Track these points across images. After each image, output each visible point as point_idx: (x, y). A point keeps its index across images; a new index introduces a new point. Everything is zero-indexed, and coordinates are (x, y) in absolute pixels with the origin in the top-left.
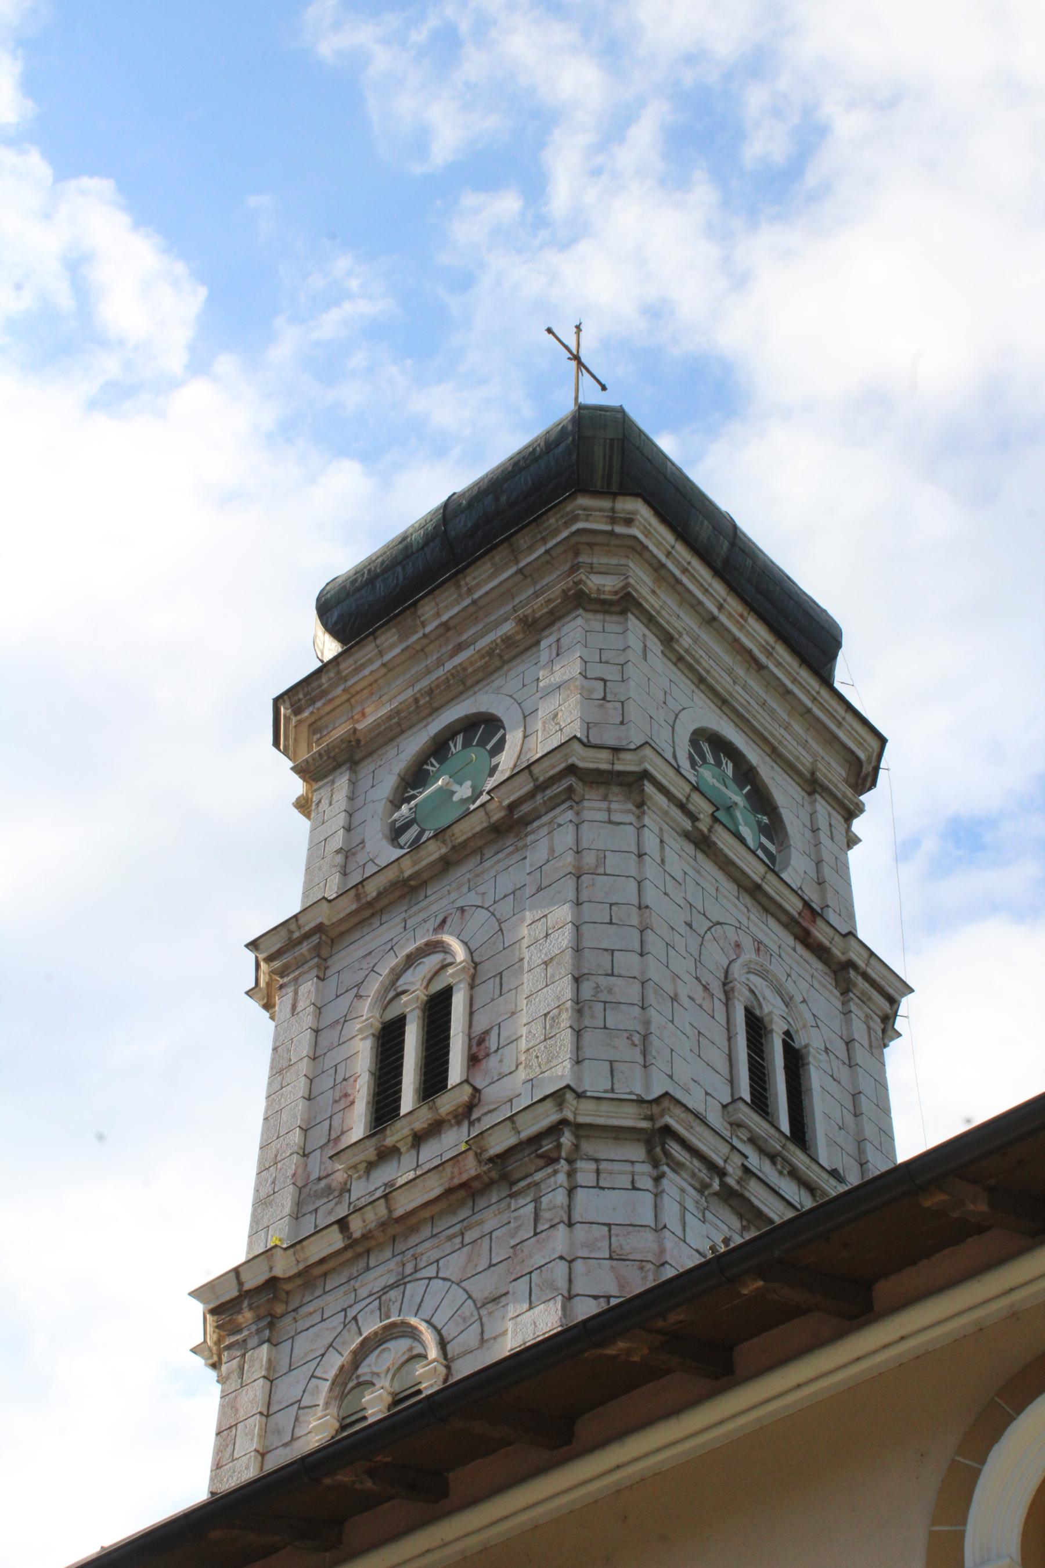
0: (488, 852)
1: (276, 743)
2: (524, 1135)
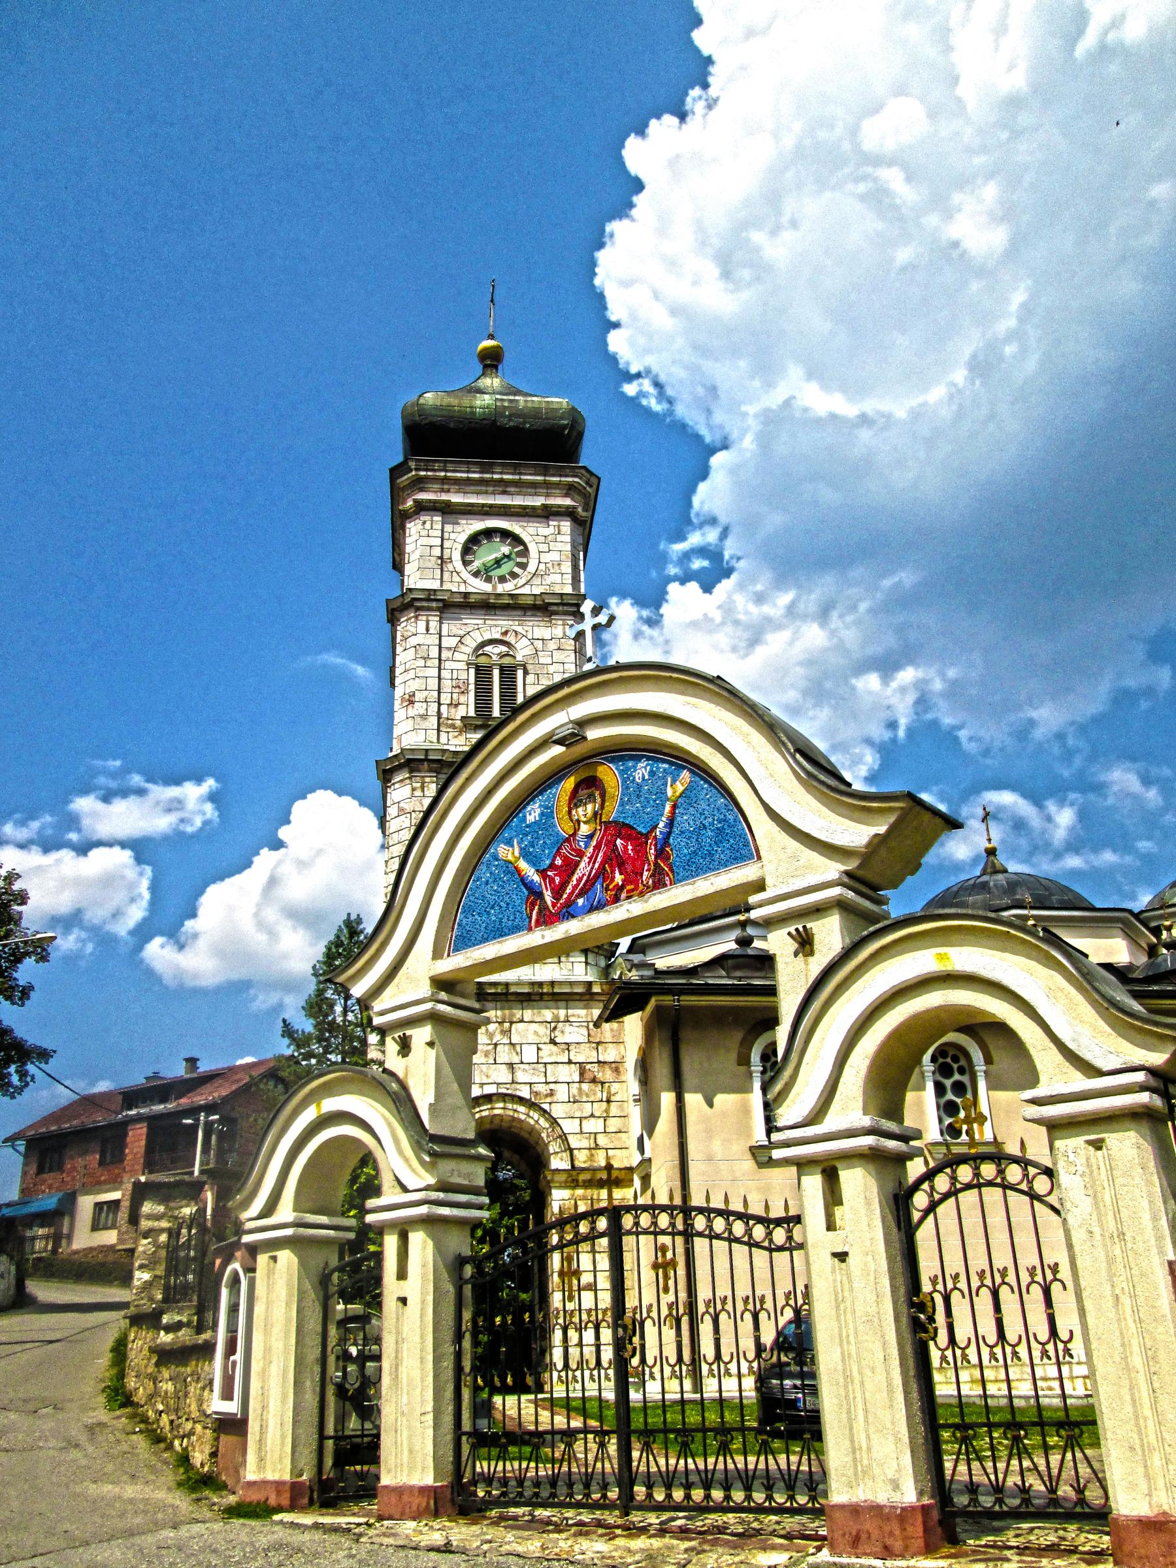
0: (529, 613)
1: (392, 470)
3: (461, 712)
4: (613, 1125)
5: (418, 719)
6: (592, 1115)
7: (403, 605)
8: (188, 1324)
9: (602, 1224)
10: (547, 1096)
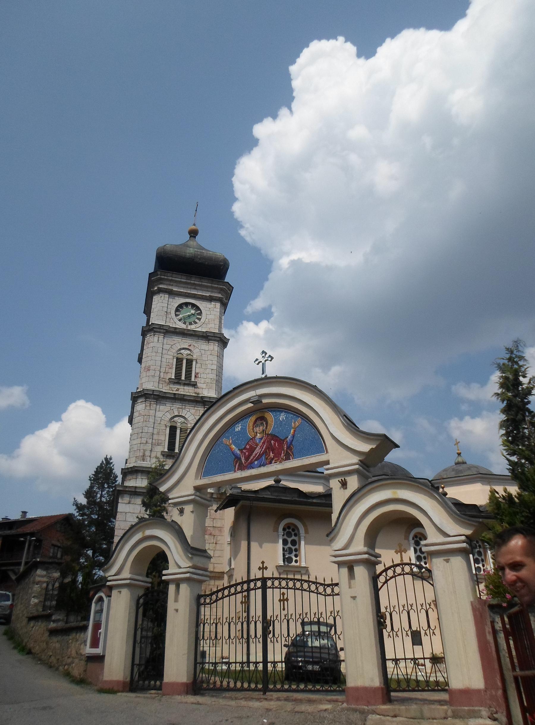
0: (200, 338)
3: (169, 376)
5: (151, 377)
7: (149, 330)
8: (63, 620)
9: (259, 584)
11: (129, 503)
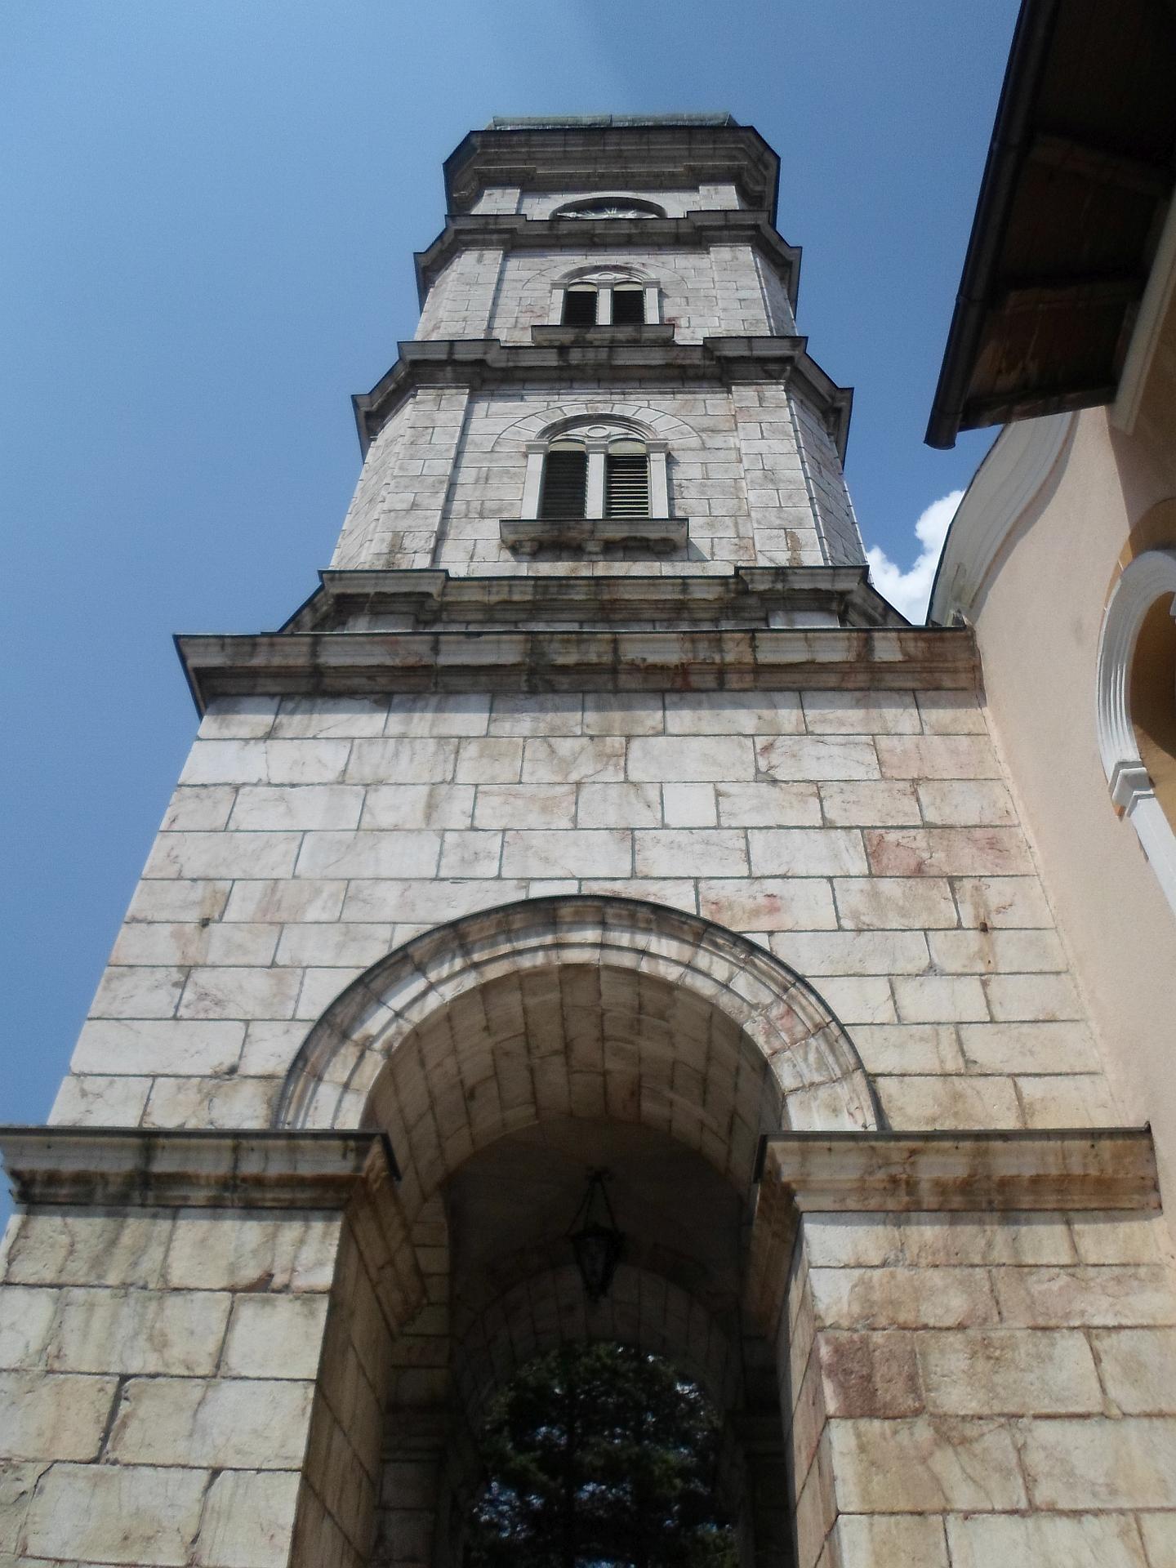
2: (756, 353)
4: (1018, 998)
6: (931, 969)
10: (756, 913)
11: (270, 735)
